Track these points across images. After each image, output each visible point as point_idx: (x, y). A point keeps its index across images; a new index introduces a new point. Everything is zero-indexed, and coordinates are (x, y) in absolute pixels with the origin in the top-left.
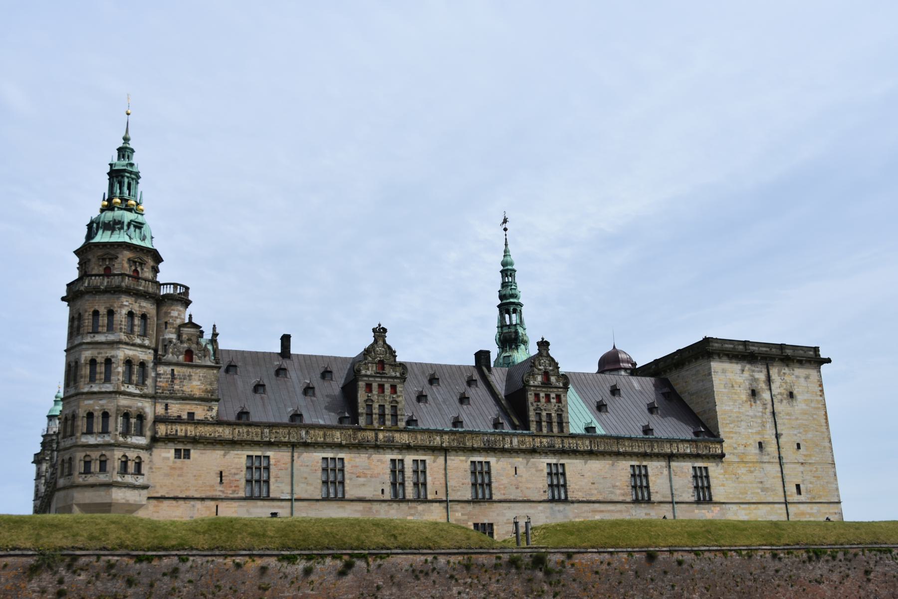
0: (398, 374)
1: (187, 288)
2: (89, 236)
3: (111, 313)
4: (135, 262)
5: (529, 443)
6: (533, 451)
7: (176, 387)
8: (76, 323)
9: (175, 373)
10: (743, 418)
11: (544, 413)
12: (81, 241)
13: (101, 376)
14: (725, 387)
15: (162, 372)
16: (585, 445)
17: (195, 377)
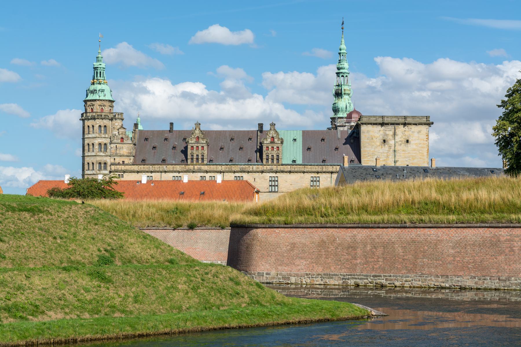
0: (205, 142)
5: (261, 168)
6: (262, 172)
7: (118, 152)
10: (376, 153)
11: (270, 155)
13: (91, 150)
14: (368, 139)
16: (288, 168)
17: (124, 148)
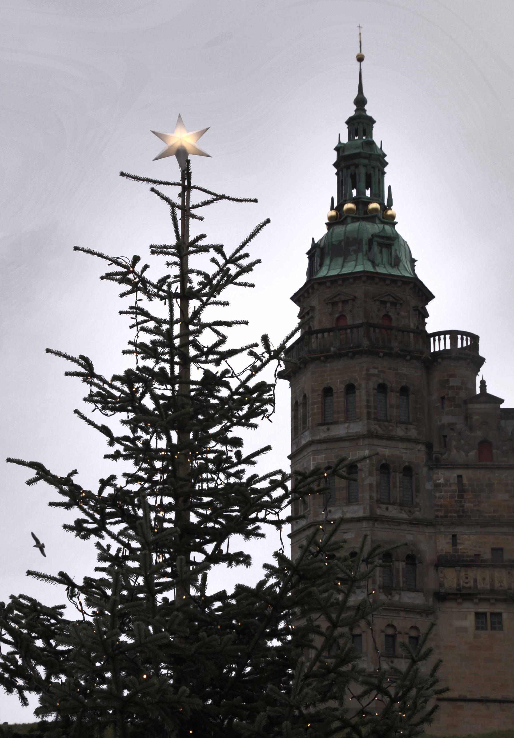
1: (475, 339)
2: (311, 271)
3: (350, 388)
4: (384, 303)
7: (468, 505)
8: (301, 411)
9: (465, 481)
12: (299, 279)
15: (442, 481)
